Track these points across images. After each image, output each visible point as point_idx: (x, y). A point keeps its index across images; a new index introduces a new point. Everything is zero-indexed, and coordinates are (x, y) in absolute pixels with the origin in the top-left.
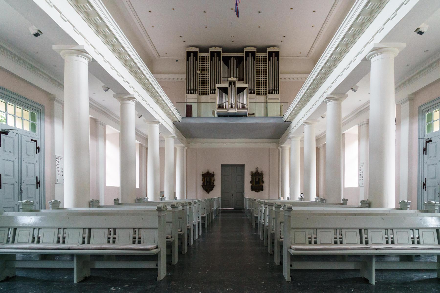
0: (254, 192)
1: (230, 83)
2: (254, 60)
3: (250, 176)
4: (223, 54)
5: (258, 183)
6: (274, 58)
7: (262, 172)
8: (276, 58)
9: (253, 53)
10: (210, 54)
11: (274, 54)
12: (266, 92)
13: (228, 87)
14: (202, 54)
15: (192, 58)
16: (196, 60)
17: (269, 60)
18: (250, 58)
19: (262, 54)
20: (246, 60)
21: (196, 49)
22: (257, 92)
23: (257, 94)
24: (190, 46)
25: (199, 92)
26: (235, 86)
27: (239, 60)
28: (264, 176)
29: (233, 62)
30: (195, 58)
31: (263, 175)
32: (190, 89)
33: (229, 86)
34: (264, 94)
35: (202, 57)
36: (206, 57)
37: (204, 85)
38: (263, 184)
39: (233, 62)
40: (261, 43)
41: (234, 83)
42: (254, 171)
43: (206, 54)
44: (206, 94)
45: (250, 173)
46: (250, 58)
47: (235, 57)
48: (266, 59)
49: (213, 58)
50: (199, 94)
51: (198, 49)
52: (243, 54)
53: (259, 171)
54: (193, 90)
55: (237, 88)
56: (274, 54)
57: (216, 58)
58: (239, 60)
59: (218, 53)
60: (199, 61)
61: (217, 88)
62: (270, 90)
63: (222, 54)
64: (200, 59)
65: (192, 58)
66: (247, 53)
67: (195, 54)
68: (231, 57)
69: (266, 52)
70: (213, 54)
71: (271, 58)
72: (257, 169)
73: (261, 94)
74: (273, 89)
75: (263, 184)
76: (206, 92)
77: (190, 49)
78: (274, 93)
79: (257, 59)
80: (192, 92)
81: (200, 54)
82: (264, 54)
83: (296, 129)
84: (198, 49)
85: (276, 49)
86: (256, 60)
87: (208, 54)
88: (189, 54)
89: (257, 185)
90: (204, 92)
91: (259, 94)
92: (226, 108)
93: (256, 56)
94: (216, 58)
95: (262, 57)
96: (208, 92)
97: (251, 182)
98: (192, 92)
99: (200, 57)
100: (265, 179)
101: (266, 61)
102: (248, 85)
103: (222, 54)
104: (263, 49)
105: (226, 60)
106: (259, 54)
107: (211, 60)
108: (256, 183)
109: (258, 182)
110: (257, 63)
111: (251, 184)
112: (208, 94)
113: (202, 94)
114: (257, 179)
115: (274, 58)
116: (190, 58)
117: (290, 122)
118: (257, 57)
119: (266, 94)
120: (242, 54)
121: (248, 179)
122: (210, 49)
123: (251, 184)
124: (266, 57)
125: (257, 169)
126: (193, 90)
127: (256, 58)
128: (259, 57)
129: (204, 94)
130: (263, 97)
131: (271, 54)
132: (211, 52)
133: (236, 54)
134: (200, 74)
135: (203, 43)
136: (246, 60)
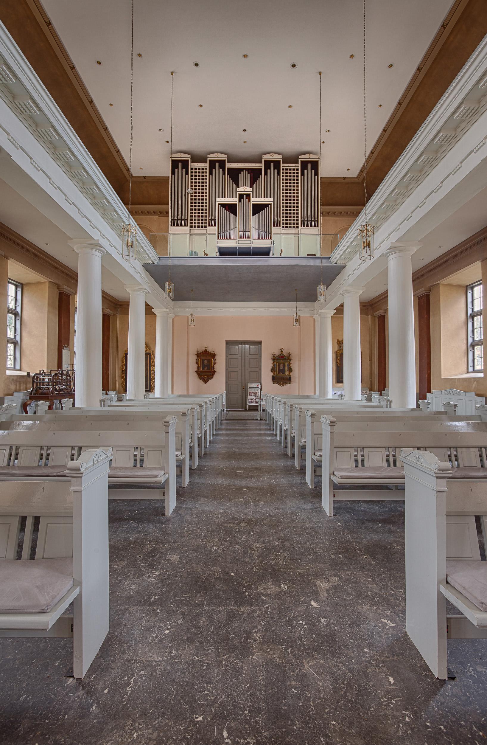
0: (276, 385)
1: (241, 196)
2: (279, 174)
3: (272, 361)
4: (229, 164)
5: (283, 371)
6: (309, 171)
7: (289, 355)
8: (313, 171)
9: (277, 164)
10: (208, 164)
11: (309, 166)
12: (297, 224)
13: (238, 203)
14: (196, 164)
15: (180, 170)
16: (187, 173)
17: (303, 174)
18: (272, 171)
19: (290, 165)
20: (266, 174)
21: (187, 157)
22: (283, 224)
23: (283, 227)
24: (178, 152)
25: (192, 223)
26: (249, 201)
27: (255, 175)
28: (291, 362)
29: (245, 177)
30: (184, 170)
31: (290, 360)
32: (176, 218)
33: (240, 201)
34: (294, 227)
35: (196, 169)
36: (203, 169)
37: (199, 213)
38: (291, 374)
39: (245, 177)
40: (290, 145)
41: (248, 196)
42: (277, 353)
43: (203, 164)
44: (202, 227)
45: (271, 357)
46: (272, 171)
47: (248, 170)
48: (297, 173)
49: (214, 170)
50: (191, 227)
51: (189, 156)
52: (262, 166)
53: (285, 353)
54: (181, 220)
55: (253, 204)
56: (309, 166)
57: (217, 171)
58: (255, 175)
59: (222, 164)
60: (192, 176)
61: (219, 204)
62: (304, 221)
63: (228, 165)
64: (192, 172)
65: (180, 170)
66: (268, 164)
67: (185, 164)
68: (242, 170)
69: (297, 163)
70: (213, 164)
71: (306, 171)
72: (282, 350)
73: (290, 227)
74: (309, 219)
75: (291, 374)
76: (202, 223)
77: (177, 157)
78: (311, 226)
79: (283, 173)
80: (179, 223)
81: (193, 164)
82: (294, 165)
83: (352, 279)
84: (189, 156)
85: (313, 157)
86: (282, 174)
87: (205, 164)
88: (175, 164)
89: (281, 375)
90: (199, 223)
91: (287, 227)
92: (235, 238)
93: (282, 168)
94: (217, 171)
95: (290, 170)
96: (206, 223)
97: (272, 370)
98: (179, 223)
99: (192, 169)
100: (295, 365)
101: (297, 176)
102: (272, 199)
103: (227, 164)
104: (292, 159)
105: (234, 175)
106: (287, 165)
107: (211, 173)
108: (280, 371)
109: (283, 370)
110: (283, 180)
111: (272, 374)
112: (206, 227)
113: (195, 227)
114: (281, 365)
115: (309, 171)
116: (176, 170)
117: (343, 266)
118: (283, 169)
119: (297, 227)
120: (260, 164)
121: (267, 365)
122: (209, 156)
123: (272, 374)
124: (297, 170)
125: (282, 350)
126: (181, 220)
127: (282, 171)
128: (287, 169)
129: (198, 227)
130: (292, 231)
131: (304, 165)
132: (210, 161)
133: (250, 164)
134: (192, 196)
135: (198, 145)
136: (266, 174)
